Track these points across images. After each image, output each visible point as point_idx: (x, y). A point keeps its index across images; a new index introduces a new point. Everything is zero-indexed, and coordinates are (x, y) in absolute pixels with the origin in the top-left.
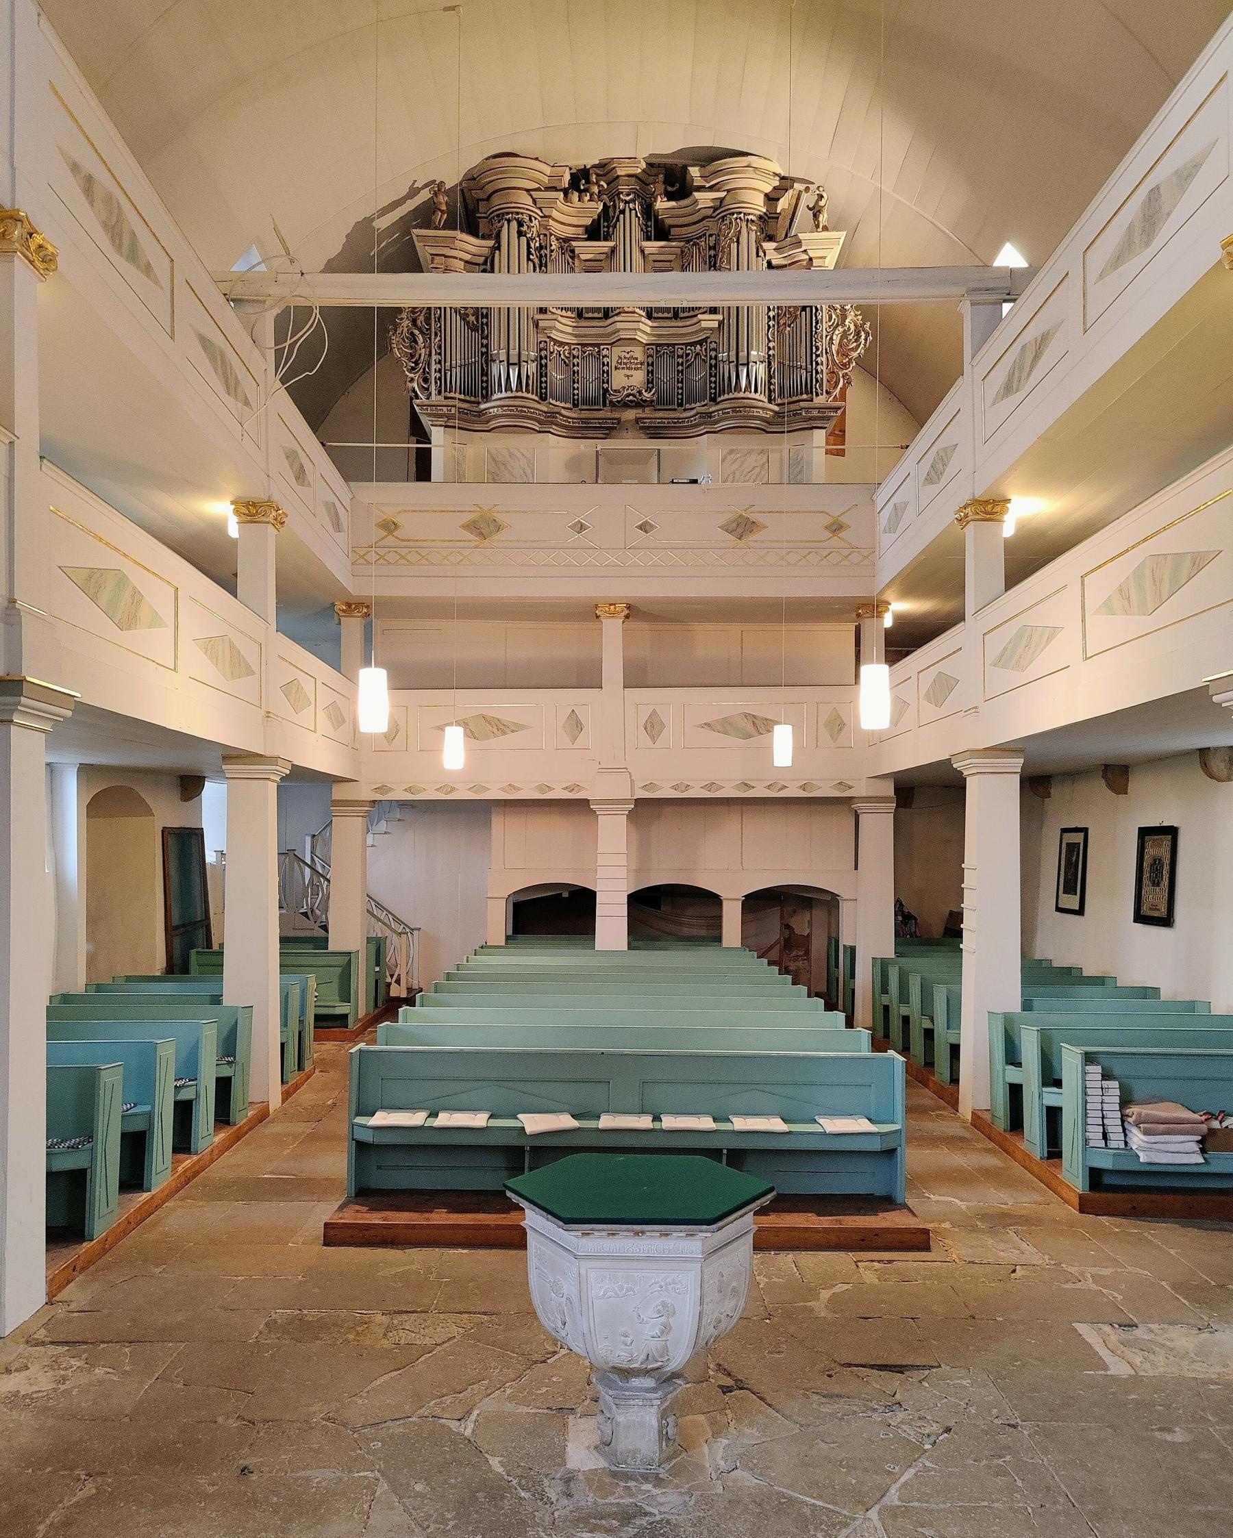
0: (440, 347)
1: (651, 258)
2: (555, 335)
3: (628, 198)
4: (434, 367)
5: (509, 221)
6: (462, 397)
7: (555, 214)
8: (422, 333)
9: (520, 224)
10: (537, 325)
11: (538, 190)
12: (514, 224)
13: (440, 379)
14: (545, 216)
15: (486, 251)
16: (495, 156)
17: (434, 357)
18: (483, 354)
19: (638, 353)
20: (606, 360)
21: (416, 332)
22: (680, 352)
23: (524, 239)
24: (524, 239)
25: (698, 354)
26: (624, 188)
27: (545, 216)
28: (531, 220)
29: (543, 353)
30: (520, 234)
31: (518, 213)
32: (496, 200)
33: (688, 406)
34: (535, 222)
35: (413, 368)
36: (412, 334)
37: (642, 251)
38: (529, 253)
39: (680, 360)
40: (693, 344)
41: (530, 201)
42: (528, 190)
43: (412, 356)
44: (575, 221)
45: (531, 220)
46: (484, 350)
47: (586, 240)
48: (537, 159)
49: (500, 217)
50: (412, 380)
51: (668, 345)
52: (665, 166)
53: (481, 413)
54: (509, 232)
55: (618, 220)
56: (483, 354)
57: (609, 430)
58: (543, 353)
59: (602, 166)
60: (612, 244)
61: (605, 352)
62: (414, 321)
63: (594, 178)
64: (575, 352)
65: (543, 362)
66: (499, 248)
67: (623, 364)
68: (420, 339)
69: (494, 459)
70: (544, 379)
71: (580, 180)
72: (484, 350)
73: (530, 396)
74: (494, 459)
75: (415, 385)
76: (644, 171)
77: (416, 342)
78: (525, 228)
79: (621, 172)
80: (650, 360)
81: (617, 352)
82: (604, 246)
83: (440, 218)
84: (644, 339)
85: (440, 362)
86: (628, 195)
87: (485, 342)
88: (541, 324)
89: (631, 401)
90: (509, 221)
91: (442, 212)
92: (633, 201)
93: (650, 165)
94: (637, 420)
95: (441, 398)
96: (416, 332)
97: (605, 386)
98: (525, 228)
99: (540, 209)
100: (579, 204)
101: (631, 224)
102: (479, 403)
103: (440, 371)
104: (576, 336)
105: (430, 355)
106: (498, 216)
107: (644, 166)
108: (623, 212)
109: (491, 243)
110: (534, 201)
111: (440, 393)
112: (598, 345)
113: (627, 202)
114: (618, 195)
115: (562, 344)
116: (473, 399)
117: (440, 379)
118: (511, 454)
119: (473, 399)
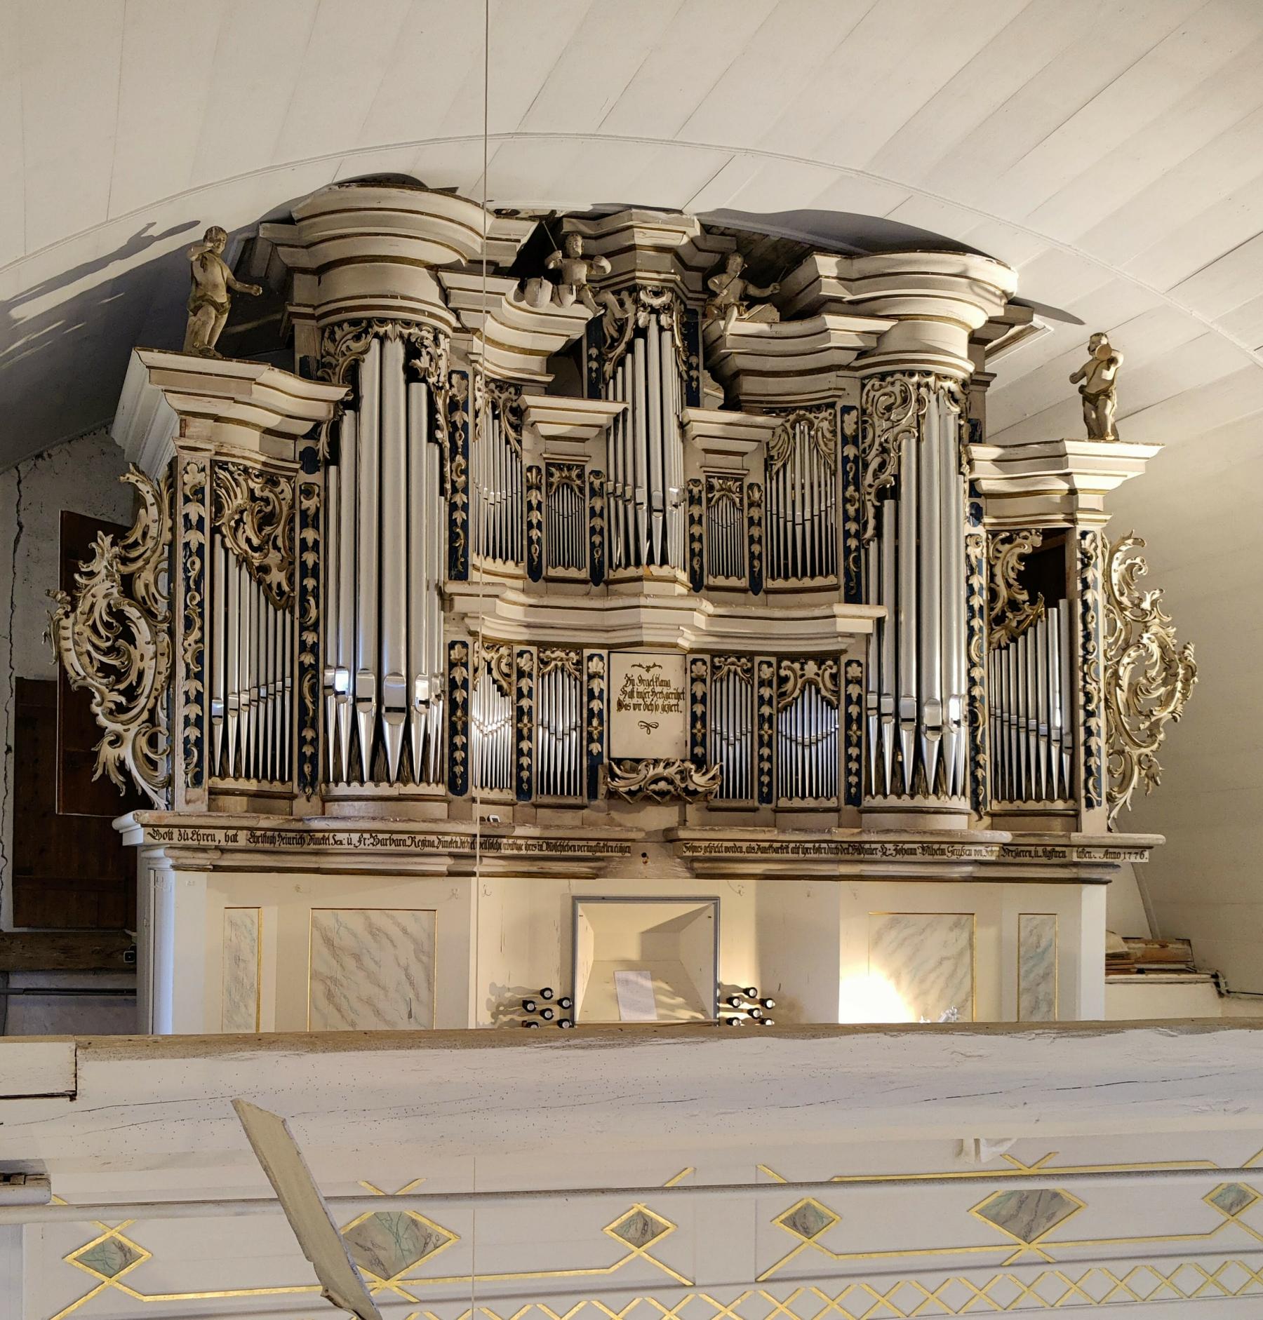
0: (199, 658)
1: (700, 444)
2: (490, 628)
3: (657, 302)
4: (183, 711)
5: (383, 339)
6: (252, 785)
7: (491, 327)
8: (149, 614)
9: (413, 351)
10: (446, 600)
11: (449, 268)
12: (396, 351)
13: (199, 742)
14: (464, 330)
15: (322, 412)
16: (365, 182)
17: (183, 685)
18: (303, 669)
19: (672, 671)
20: (597, 685)
21: (133, 612)
22: (767, 672)
23: (419, 390)
24: (419, 390)
25: (811, 682)
26: (648, 278)
27: (464, 330)
28: (436, 339)
29: (459, 674)
30: (412, 375)
31: (407, 324)
32: (347, 284)
33: (783, 802)
34: (444, 343)
35: (121, 709)
36: (120, 616)
37: (682, 426)
38: (433, 425)
39: (766, 692)
40: (793, 657)
41: (433, 294)
42: (434, 269)
43: (120, 675)
44: (527, 341)
45: (436, 339)
46: (308, 659)
47: (550, 390)
48: (450, 192)
49: (362, 328)
50: (117, 741)
51: (739, 654)
52: (735, 235)
53: (304, 836)
54: (381, 366)
55: (630, 348)
56: (303, 669)
57: (600, 857)
58: (459, 674)
59: (595, 217)
60: (618, 408)
61: (595, 666)
62: (127, 584)
63: (578, 246)
64: (524, 663)
65: (459, 695)
66: (353, 404)
67: (640, 696)
68: (142, 630)
69: (329, 942)
70: (459, 740)
71: (540, 254)
72: (308, 659)
73: (423, 789)
74: (329, 942)
75: (126, 752)
76: (692, 241)
77: (131, 640)
78: (423, 363)
79: (641, 238)
80: (699, 689)
81: (622, 665)
82: (601, 410)
83: (212, 324)
84: (687, 640)
85: (199, 699)
86: (657, 294)
87: (310, 638)
88: (460, 604)
89: (662, 794)
90: (383, 339)
91: (219, 307)
92: (667, 308)
93: (707, 229)
94: (668, 838)
95: (201, 793)
96: (133, 612)
97: (595, 747)
98: (423, 363)
99: (455, 311)
100: (554, 309)
101: (658, 361)
102: (291, 797)
103: (199, 722)
104: (528, 626)
105: (171, 677)
106: (354, 322)
107: (696, 231)
108: (641, 332)
109: (339, 393)
110: (445, 294)
111: (197, 780)
112: (578, 648)
113: (654, 311)
114: (634, 290)
115: (493, 645)
116: (277, 787)
117: (199, 742)
118: (374, 931)
119: (277, 787)
